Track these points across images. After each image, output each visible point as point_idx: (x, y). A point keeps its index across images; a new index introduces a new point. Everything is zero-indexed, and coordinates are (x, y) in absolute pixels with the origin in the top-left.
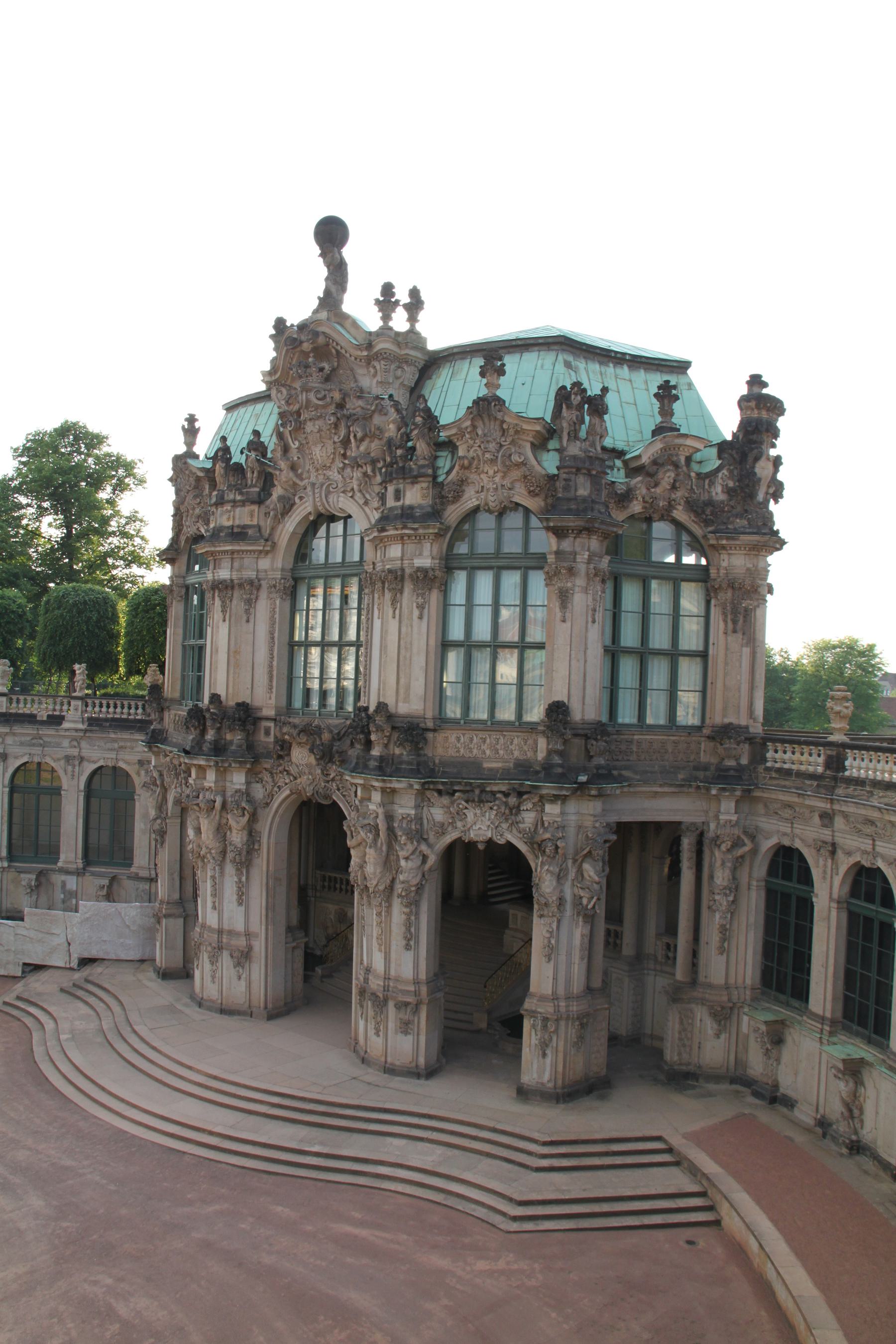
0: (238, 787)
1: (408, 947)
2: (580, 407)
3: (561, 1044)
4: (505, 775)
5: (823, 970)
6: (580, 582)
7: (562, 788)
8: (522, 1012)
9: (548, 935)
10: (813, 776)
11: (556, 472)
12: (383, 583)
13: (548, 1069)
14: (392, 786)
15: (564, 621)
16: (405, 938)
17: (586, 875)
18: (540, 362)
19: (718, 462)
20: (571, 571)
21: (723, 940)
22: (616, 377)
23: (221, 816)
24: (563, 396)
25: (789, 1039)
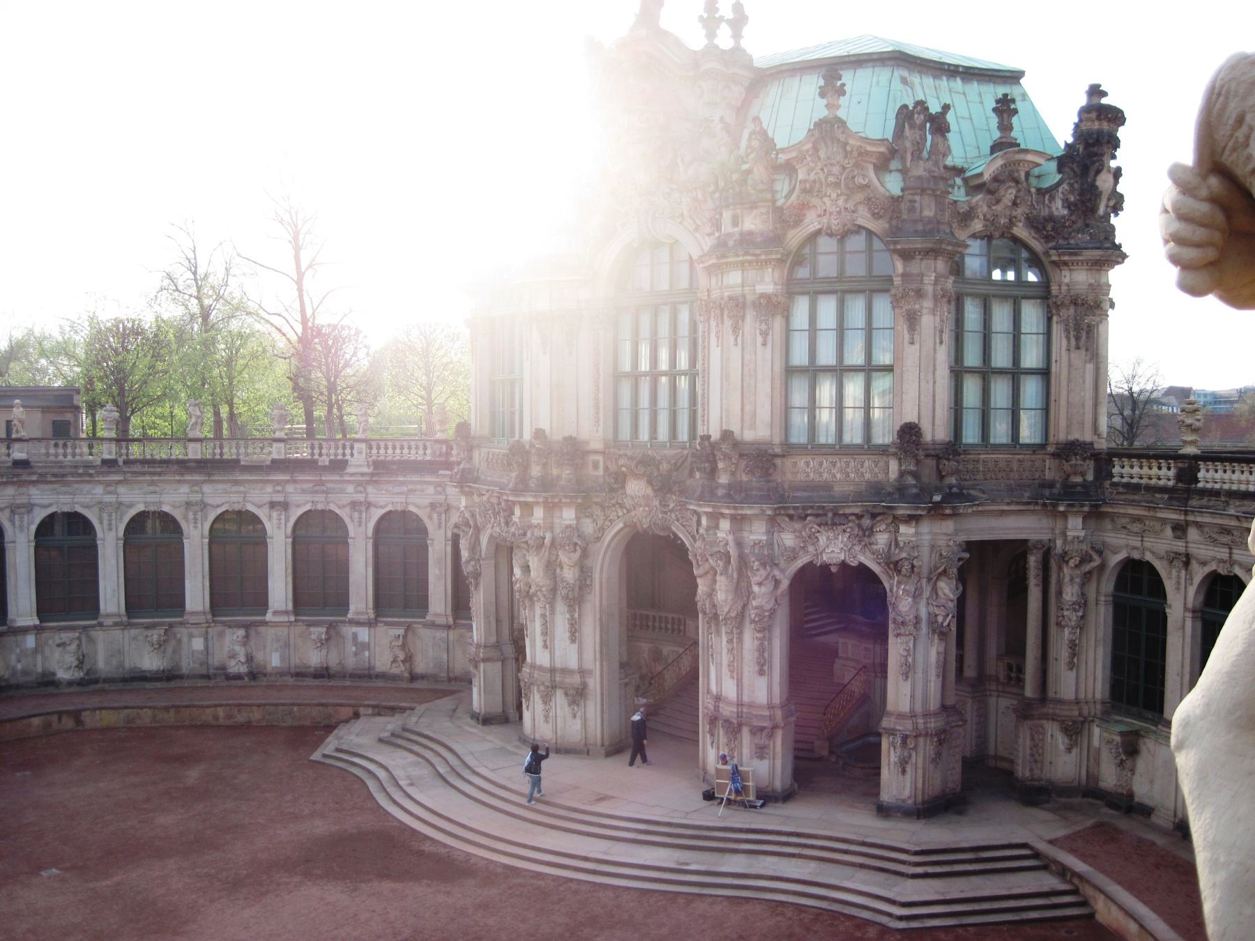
0: (568, 522)
1: (761, 672)
2: (922, 127)
3: (920, 760)
4: (858, 497)
5: (1178, 679)
6: (928, 303)
7: (917, 508)
8: (880, 730)
9: (905, 654)
10: (1163, 490)
11: (901, 194)
12: (722, 310)
13: (908, 785)
14: (744, 512)
15: (912, 343)
16: (758, 663)
17: (940, 593)
18: (875, 79)
19: (1059, 177)
20: (920, 294)
21: (1073, 655)
22: (950, 91)
23: (550, 553)
24: (905, 115)
25: (1143, 749)
